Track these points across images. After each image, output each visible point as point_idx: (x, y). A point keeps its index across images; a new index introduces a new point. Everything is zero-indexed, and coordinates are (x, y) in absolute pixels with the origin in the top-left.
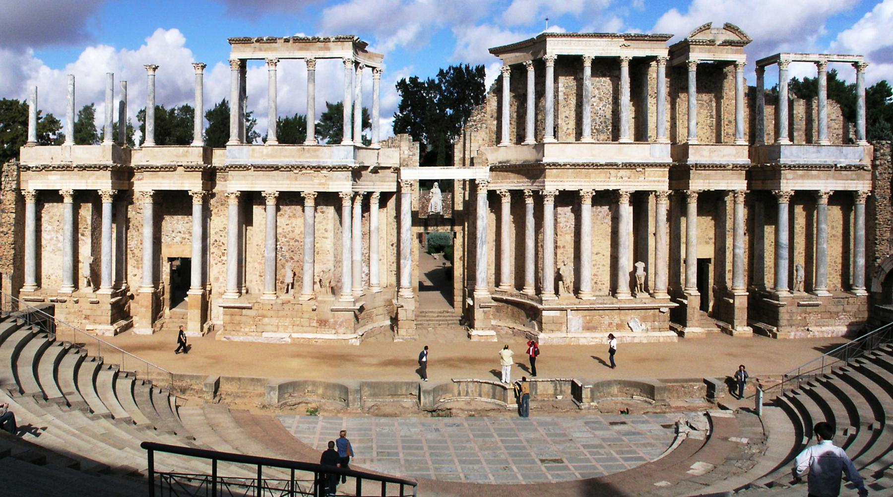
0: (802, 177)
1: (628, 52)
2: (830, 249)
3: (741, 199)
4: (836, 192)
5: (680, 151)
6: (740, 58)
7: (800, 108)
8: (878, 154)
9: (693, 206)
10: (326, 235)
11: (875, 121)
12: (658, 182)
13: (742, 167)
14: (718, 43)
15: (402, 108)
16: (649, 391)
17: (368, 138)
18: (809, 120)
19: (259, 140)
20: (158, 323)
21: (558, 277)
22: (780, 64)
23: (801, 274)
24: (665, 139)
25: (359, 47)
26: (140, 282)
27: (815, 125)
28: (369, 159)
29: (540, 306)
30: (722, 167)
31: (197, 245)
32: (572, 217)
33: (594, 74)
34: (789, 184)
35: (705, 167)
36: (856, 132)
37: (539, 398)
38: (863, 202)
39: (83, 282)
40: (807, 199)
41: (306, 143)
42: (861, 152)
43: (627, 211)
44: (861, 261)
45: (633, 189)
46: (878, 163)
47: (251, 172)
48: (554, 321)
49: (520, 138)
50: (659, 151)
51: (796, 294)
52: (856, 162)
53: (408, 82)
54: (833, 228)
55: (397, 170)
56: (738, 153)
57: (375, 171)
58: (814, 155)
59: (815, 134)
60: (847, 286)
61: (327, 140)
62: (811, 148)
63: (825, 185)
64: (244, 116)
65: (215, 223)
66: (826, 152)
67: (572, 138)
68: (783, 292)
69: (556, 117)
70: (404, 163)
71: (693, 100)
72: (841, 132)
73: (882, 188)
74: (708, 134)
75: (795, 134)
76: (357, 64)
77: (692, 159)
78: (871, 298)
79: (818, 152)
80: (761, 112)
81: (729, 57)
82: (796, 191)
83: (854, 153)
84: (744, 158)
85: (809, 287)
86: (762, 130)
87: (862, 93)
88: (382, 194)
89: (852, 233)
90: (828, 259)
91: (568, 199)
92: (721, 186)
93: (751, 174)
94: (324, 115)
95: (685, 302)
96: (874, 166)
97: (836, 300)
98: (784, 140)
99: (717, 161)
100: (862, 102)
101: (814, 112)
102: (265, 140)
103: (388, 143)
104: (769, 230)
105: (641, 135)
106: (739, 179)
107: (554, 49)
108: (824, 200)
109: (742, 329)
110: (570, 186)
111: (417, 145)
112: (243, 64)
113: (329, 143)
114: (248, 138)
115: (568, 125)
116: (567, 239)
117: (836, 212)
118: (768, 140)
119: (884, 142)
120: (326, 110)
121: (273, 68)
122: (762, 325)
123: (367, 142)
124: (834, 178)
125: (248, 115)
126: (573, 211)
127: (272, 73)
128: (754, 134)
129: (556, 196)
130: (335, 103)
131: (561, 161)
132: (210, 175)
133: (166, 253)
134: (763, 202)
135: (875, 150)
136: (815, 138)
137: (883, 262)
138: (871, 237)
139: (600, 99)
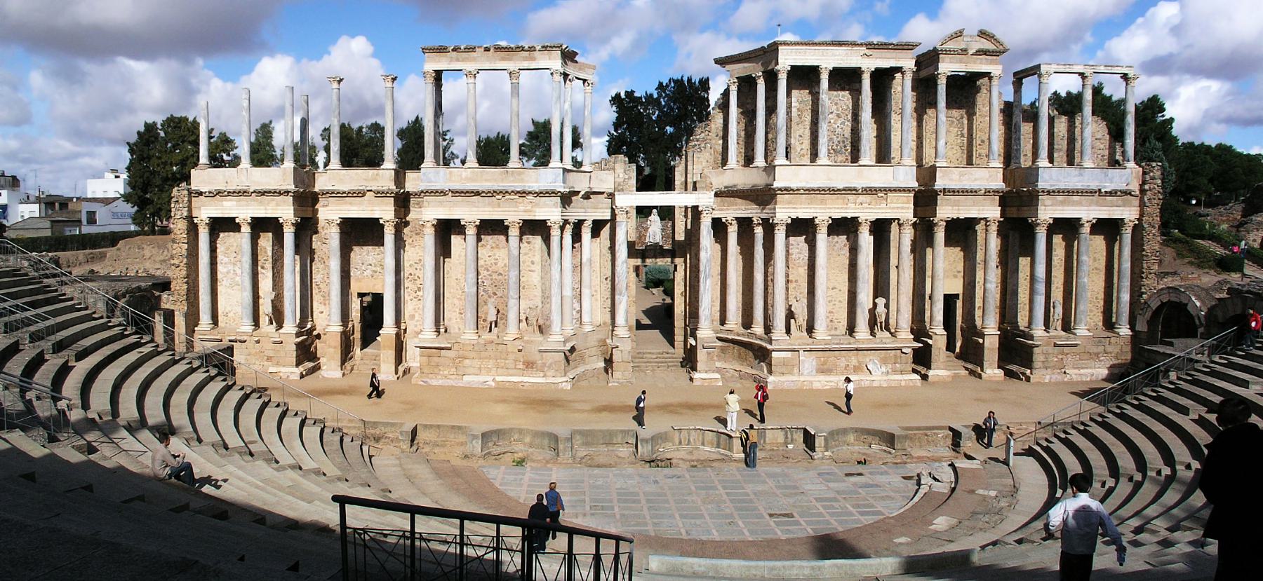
0: (1062, 203)
1: (870, 63)
2: (1091, 283)
3: (994, 228)
4: (1099, 220)
5: (927, 174)
6: (995, 69)
7: (1061, 125)
8: (1148, 177)
9: (940, 235)
10: (533, 268)
11: (1144, 141)
12: (902, 209)
13: (996, 192)
14: (971, 52)
15: (617, 125)
16: (889, 439)
17: (579, 159)
18: (1071, 140)
19: (458, 161)
20: (348, 365)
21: (790, 315)
22: (1040, 76)
23: (1058, 312)
24: (910, 160)
25: (569, 56)
26: (327, 319)
27: (1078, 145)
28: (580, 183)
29: (769, 347)
30: (973, 192)
31: (390, 279)
32: (806, 247)
33: (831, 88)
34: (1048, 212)
35: (954, 192)
36: (1124, 153)
37: (768, 447)
38: (1129, 230)
40: (1067, 228)
41: (510, 165)
42: (1129, 175)
43: (866, 240)
44: (1126, 297)
45: (873, 217)
46: (1147, 187)
47: (449, 197)
48: (784, 363)
49: (749, 160)
50: (904, 174)
51: (1052, 333)
52: (1124, 187)
53: (623, 96)
54: (1095, 260)
55: (611, 196)
56: (991, 177)
57: (587, 196)
58: (1076, 179)
59: (1077, 155)
60: (1109, 325)
61: (533, 161)
62: (1072, 171)
63: (1087, 212)
64: (440, 135)
65: (409, 255)
66: (1090, 174)
67: (807, 160)
68: (1038, 331)
69: (788, 135)
70: (619, 188)
71: (942, 117)
72: (1106, 152)
73: (1150, 215)
74: (959, 155)
75: (1056, 155)
76: (565, 76)
77: (940, 184)
78: (1136, 338)
79: (1081, 175)
80: (1018, 130)
82: (1055, 219)
83: (1121, 176)
84: (998, 184)
85: (1067, 326)
86: (1018, 150)
87: (1131, 109)
88: (594, 221)
89: (1116, 266)
90: (1089, 294)
91: (802, 227)
92: (973, 213)
93: (1005, 200)
94: (530, 133)
95: (930, 342)
96: (1143, 191)
97: (1097, 341)
98: (1043, 162)
99: (968, 184)
100: (1130, 119)
101: (1077, 131)
102: (463, 162)
103: (600, 165)
104: (1024, 262)
105: (883, 156)
106: (992, 205)
107: (787, 59)
108: (1086, 229)
109: (992, 371)
110: (804, 213)
111: (634, 167)
112: (438, 76)
113: (535, 165)
114: (445, 160)
115: (801, 145)
116: (801, 273)
117: (1099, 242)
118: (1025, 162)
119: (1154, 164)
120: (532, 128)
121: (472, 80)
122: (1012, 367)
123: (577, 164)
124: (1098, 204)
125: (445, 134)
126: (806, 241)
127: (471, 86)
128: (1009, 156)
129: (788, 225)
130: (542, 120)
131: (794, 186)
132: (403, 202)
133: (355, 288)
134: (1018, 232)
135: (1144, 173)
136: (1077, 160)
137: (1150, 298)
138: (1137, 270)
139: (838, 116)
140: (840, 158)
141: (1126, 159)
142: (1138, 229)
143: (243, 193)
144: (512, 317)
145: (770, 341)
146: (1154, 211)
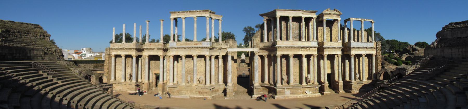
3: (340, 57)
6: (339, 19)
12: (314, 52)
30: (334, 48)
31: (161, 70)
33: (292, 21)
34: (353, 52)
39: (127, 79)
40: (358, 56)
43: (305, 60)
48: (280, 92)
50: (315, 44)
57: (220, 49)
63: (364, 52)
66: (364, 44)
71: (325, 30)
77: (325, 46)
81: (336, 18)
84: (340, 45)
92: (334, 53)
99: (332, 46)
107: (279, 14)
116: (284, 69)
140: (296, 40)
141: (372, 40)
142: (376, 56)
143: (122, 49)
144: (195, 79)
145: (276, 87)
146: (380, 52)
